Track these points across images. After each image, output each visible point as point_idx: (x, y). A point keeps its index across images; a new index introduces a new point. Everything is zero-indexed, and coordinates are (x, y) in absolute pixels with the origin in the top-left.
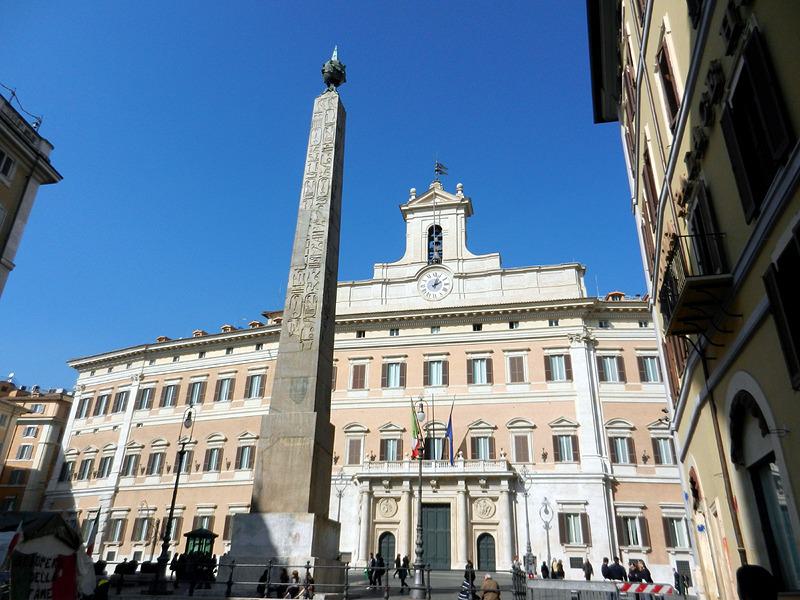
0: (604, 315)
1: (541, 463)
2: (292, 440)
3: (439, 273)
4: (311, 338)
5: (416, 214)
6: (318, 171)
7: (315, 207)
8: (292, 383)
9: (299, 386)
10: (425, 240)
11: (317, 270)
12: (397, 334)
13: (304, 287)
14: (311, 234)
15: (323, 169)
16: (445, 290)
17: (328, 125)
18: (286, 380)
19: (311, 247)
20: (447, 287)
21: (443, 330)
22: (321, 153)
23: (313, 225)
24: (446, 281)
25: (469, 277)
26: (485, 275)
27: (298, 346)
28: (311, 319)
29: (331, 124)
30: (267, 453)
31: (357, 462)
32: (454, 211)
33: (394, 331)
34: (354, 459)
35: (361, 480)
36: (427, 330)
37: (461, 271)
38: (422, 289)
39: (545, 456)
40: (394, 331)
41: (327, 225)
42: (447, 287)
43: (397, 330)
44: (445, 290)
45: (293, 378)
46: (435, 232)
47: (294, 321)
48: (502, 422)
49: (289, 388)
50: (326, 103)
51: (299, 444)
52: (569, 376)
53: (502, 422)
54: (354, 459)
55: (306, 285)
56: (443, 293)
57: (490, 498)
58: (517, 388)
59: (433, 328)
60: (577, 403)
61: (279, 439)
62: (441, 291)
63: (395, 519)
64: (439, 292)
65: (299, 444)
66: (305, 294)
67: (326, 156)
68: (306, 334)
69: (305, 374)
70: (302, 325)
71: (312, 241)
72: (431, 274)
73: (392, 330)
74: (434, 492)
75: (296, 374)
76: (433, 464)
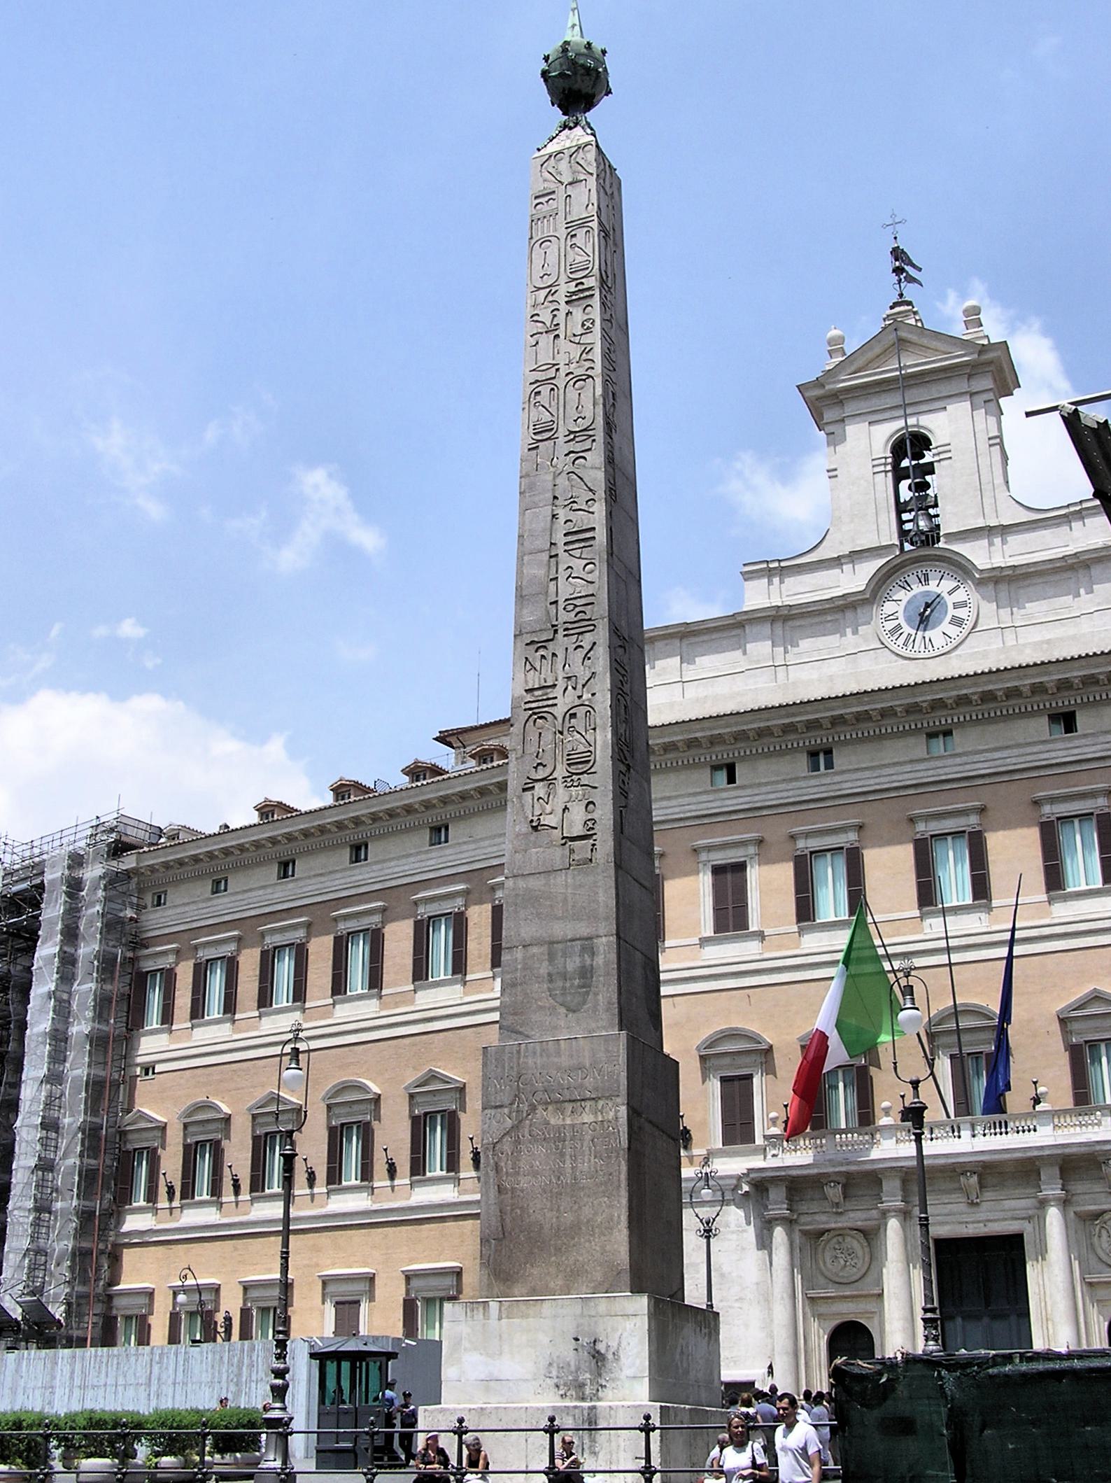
2: (569, 1107)
4: (590, 824)
5: (850, 408)
6: (562, 359)
7: (562, 463)
8: (551, 957)
9: (573, 964)
11: (587, 640)
12: (829, 765)
13: (558, 692)
14: (560, 539)
15: (576, 352)
16: (957, 621)
17: (573, 227)
18: (535, 950)
19: (562, 575)
20: (962, 613)
21: (962, 741)
22: (564, 308)
23: (563, 514)
24: (960, 595)
25: (1027, 576)
26: (1071, 568)
27: (558, 856)
28: (585, 779)
29: (583, 223)
30: (507, 1146)
32: (963, 385)
33: (820, 756)
34: (738, 1128)
35: (760, 1187)
36: (917, 746)
37: (998, 561)
38: (890, 625)
40: (820, 756)
41: (600, 509)
42: (962, 613)
43: (828, 752)
45: (552, 943)
47: (540, 789)
49: (544, 969)
50: (564, 165)
51: (588, 1118)
54: (738, 1128)
55: (561, 684)
56: (953, 631)
59: (931, 735)
61: (533, 1108)
62: (945, 626)
65: (588, 1118)
66: (559, 711)
67: (578, 315)
68: (576, 822)
69: (583, 929)
70: (561, 794)
71: (563, 556)
73: (813, 755)
74: (972, 1204)
75: (561, 930)
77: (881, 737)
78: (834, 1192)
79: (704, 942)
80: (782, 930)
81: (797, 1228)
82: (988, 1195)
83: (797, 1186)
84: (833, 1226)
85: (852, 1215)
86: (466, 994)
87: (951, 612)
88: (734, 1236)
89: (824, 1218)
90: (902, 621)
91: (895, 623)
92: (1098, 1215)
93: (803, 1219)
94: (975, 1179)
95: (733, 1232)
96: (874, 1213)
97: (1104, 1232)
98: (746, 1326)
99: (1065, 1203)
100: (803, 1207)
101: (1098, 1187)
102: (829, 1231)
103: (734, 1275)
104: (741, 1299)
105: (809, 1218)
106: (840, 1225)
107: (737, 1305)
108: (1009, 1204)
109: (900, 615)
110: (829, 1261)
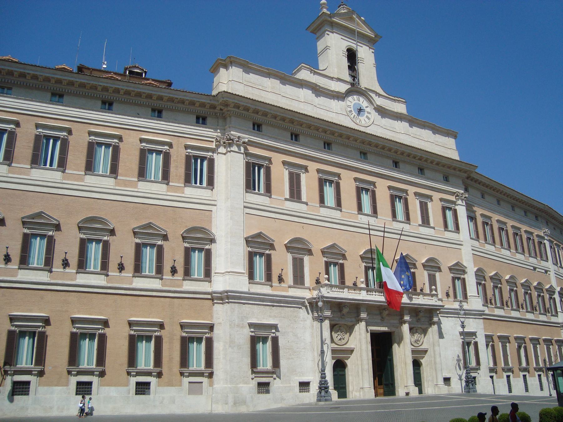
0: (469, 182)
1: (445, 299)
3: (361, 99)
10: (345, 60)
20: (369, 115)
34: (299, 279)
38: (349, 109)
39: (448, 295)
42: (369, 115)
44: (367, 117)
46: (352, 56)
52: (457, 228)
58: (424, 231)
60: (463, 251)
63: (347, 346)
64: (363, 119)
72: (355, 97)
77: (347, 146)
79: (286, 199)
80: (314, 204)
83: (337, 306)
84: (340, 322)
86: (168, 191)
87: (366, 114)
88: (302, 323)
89: (337, 319)
90: (352, 109)
91: (350, 109)
107: (303, 350)
108: (392, 321)
109: (352, 107)
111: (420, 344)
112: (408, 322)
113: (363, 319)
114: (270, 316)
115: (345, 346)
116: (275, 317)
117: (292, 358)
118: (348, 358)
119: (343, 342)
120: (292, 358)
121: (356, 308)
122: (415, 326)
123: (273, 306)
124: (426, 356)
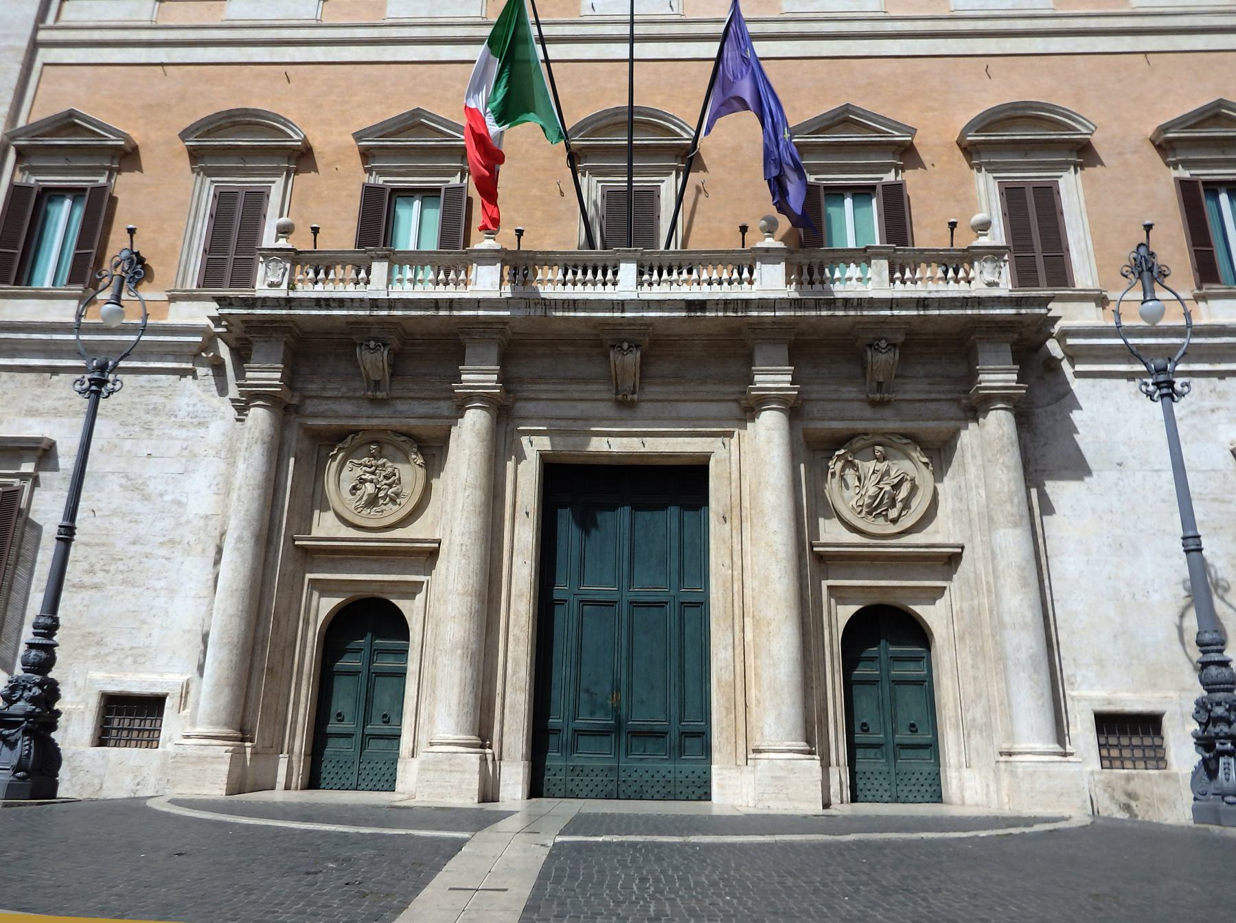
31: (245, 277)
48: (939, 124)
53: (939, 124)
57: (905, 436)
76: (628, 271)
78: (374, 361)
81: (295, 420)
82: (653, 391)
84: (363, 422)
85: (401, 406)
88: (183, 433)
89: (348, 408)
92: (842, 440)
93: (310, 406)
94: (634, 358)
95: (181, 426)
96: (445, 407)
97: (850, 475)
98: (171, 592)
99: (794, 411)
100: (313, 387)
101: (850, 391)
102: (355, 432)
103: (168, 498)
104: (172, 542)
105: (323, 406)
106: (375, 422)
107: (163, 552)
110: (346, 486)
111: (907, 522)
112: (781, 400)
113: (470, 398)
114: (32, 413)
115: (397, 533)
116: (56, 413)
117: (95, 587)
118: (412, 590)
119: (393, 513)
120: (95, 587)
121: (424, 350)
122: (860, 425)
123: (55, 371)
124: (955, 586)
